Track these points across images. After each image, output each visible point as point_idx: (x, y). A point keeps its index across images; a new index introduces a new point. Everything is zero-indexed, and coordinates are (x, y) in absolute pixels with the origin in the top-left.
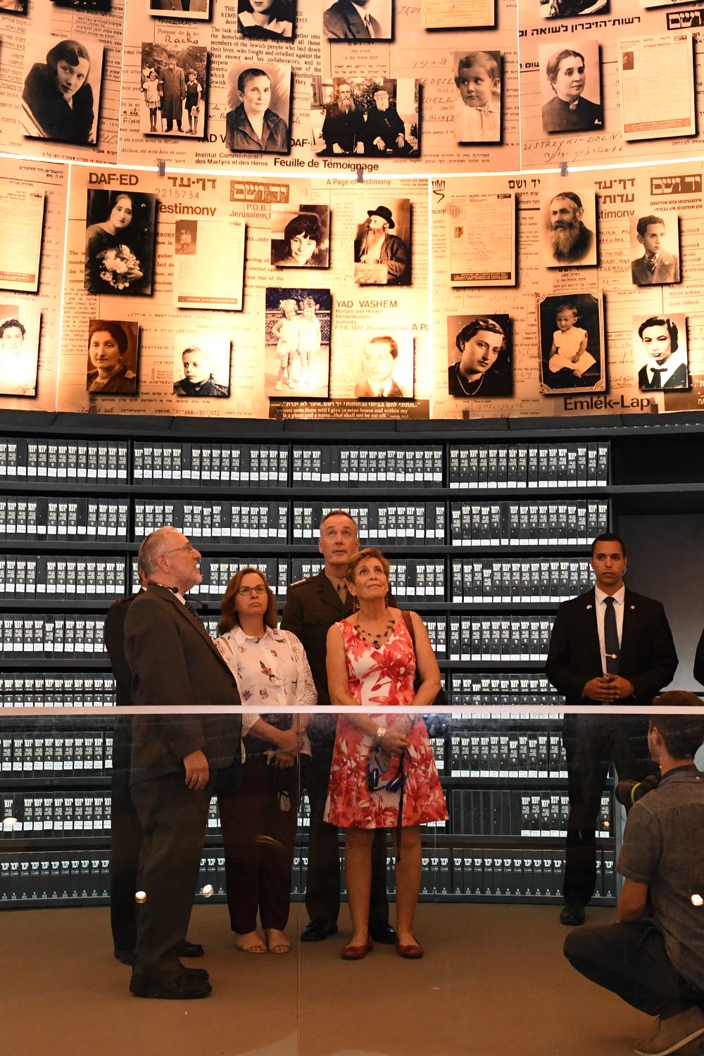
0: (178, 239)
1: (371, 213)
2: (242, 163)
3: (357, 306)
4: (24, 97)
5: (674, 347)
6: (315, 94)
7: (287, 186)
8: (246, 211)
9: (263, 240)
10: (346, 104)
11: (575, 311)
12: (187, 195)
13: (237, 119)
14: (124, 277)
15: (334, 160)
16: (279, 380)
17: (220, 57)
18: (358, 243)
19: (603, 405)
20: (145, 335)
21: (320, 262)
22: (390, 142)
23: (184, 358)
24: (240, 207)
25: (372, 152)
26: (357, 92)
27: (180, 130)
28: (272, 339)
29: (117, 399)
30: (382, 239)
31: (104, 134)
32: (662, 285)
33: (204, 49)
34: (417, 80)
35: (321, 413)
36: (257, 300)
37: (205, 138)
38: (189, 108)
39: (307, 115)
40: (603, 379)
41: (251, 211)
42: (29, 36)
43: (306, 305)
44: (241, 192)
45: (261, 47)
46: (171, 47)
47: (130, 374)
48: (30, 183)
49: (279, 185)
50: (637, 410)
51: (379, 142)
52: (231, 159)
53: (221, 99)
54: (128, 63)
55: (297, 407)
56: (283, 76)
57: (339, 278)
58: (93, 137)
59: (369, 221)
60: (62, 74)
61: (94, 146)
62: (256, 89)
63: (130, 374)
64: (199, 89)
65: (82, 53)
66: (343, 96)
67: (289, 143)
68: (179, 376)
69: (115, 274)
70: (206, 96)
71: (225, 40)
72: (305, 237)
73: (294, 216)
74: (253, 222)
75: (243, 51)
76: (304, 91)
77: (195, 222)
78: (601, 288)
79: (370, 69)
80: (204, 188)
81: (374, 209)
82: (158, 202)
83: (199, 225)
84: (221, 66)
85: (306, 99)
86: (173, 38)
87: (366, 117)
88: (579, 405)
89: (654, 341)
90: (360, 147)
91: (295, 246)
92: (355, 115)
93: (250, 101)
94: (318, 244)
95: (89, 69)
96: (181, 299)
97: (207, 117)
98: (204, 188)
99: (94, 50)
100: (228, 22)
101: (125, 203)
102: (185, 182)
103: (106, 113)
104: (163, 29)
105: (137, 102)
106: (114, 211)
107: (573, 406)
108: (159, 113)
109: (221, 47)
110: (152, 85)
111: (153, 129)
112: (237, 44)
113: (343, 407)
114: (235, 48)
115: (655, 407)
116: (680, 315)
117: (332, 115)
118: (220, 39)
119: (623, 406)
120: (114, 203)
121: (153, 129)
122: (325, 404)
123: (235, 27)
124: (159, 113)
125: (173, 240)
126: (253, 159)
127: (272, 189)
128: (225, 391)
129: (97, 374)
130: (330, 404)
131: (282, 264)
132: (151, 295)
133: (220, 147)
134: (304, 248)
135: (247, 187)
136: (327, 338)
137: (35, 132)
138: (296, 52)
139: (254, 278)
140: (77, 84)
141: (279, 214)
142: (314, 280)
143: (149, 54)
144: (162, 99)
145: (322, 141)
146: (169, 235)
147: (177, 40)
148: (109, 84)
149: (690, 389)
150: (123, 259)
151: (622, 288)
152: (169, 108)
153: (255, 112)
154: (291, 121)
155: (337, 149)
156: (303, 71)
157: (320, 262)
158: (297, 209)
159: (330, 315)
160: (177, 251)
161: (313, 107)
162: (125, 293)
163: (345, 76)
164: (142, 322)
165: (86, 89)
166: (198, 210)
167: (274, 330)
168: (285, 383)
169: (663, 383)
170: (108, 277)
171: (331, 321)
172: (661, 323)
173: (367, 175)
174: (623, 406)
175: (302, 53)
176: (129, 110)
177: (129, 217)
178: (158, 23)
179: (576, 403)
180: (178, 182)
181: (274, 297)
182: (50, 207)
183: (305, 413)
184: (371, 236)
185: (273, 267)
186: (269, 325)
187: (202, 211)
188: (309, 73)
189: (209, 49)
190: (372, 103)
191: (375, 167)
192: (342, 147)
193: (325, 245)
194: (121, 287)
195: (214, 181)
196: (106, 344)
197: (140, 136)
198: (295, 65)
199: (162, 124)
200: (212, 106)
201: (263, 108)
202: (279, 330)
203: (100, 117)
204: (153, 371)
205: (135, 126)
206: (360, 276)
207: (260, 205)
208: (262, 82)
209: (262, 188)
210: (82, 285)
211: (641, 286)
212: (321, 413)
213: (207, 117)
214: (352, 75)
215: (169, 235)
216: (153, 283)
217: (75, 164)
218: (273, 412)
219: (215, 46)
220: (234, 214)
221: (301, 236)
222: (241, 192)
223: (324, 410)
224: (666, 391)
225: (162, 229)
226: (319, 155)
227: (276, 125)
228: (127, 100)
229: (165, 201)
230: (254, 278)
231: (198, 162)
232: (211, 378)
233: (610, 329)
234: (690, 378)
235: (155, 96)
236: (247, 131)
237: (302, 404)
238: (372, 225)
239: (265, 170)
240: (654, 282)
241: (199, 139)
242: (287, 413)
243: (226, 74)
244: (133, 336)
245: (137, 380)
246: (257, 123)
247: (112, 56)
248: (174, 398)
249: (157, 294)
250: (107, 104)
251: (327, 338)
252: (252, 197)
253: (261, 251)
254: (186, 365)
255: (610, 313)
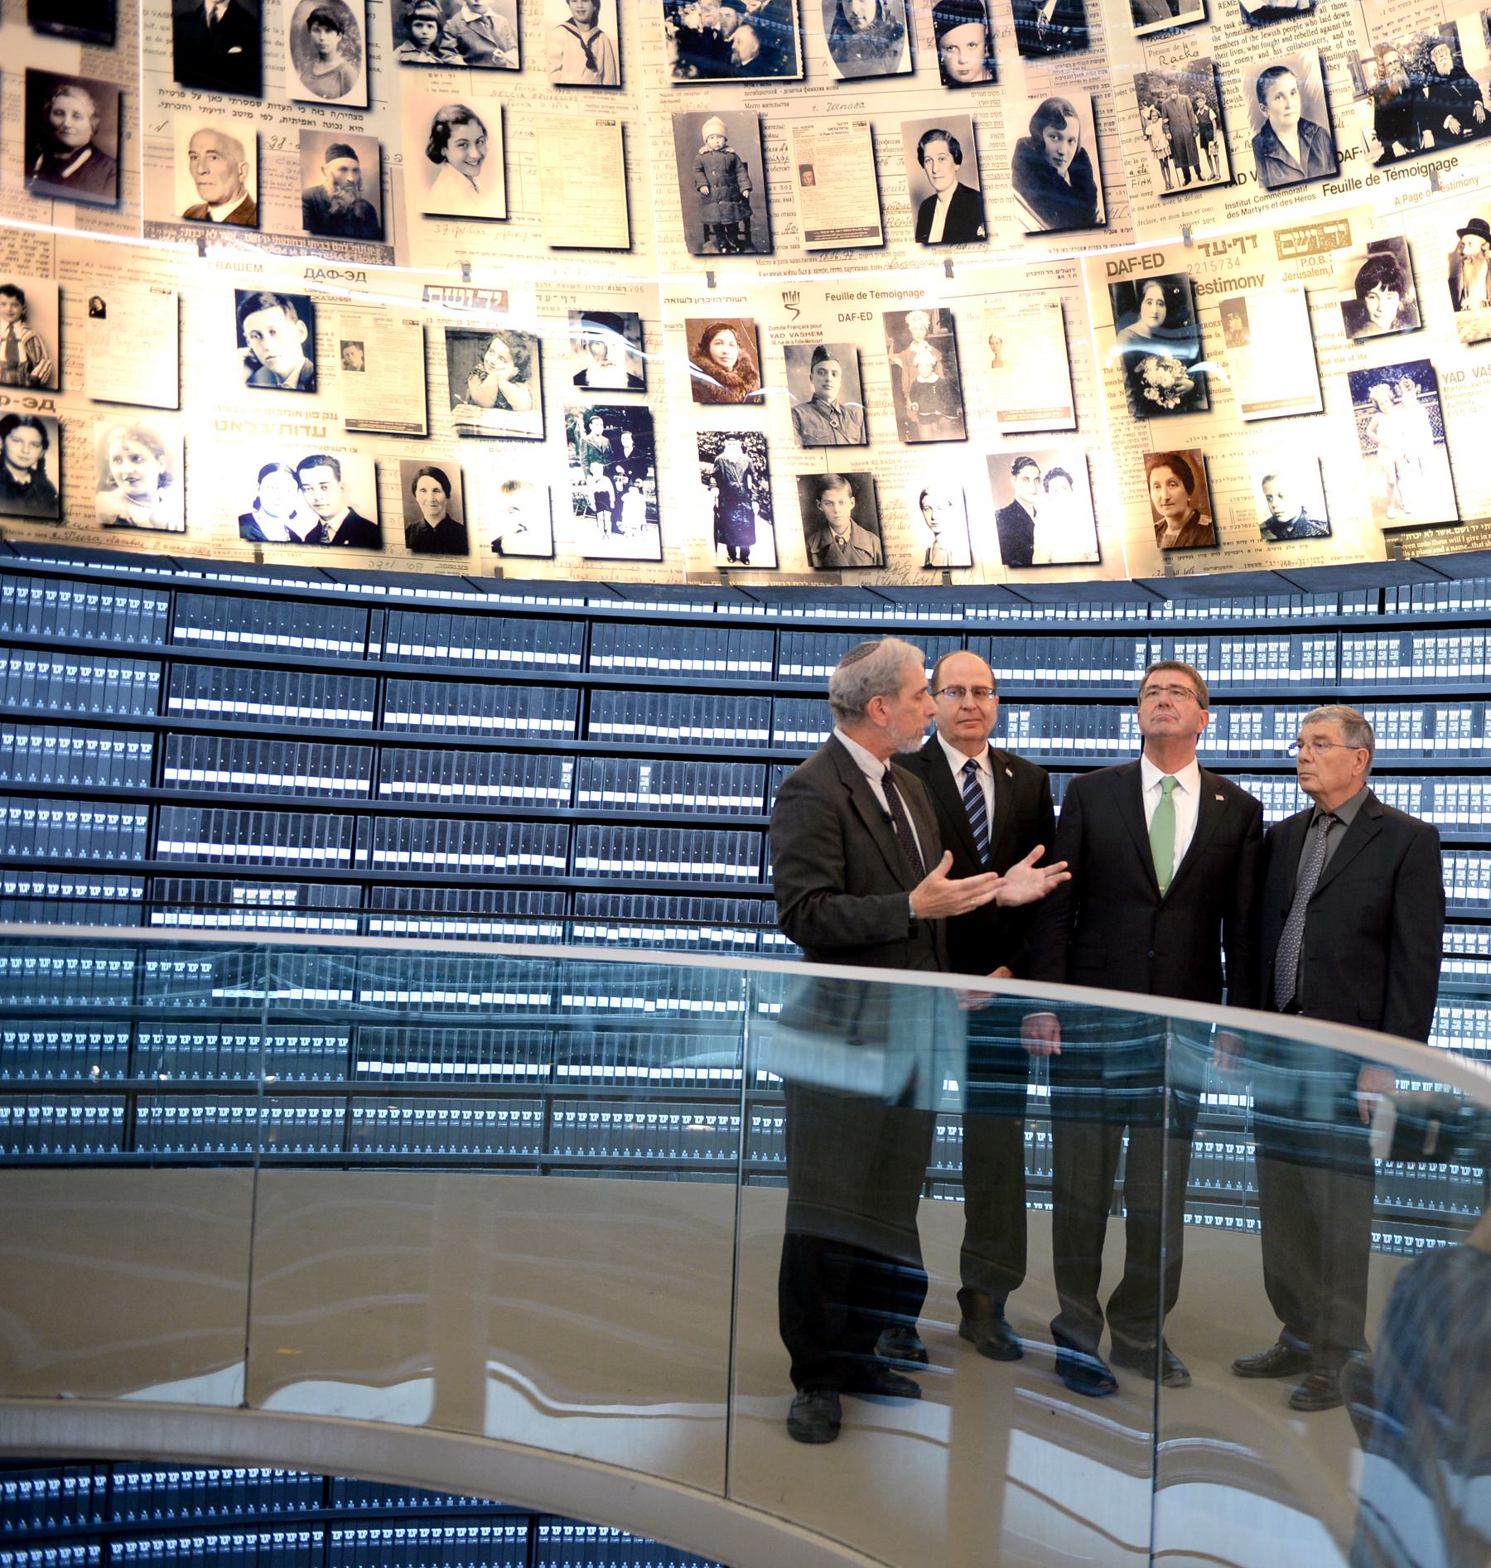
0: (1226, 328)
1: (1462, 233)
2: (1284, 203)
3: (1470, 378)
4: (1015, 185)
6: (1355, 79)
7: (1345, 221)
8: (1302, 270)
9: (1330, 305)
10: (1397, 80)
12: (1226, 264)
13: (1266, 143)
14: (1173, 390)
15: (1398, 167)
16: (1389, 503)
17: (1228, 63)
18: (1453, 282)
20: (1212, 464)
21: (1409, 319)
22: (1466, 119)
23: (1265, 489)
24: (1292, 265)
25: (1446, 140)
26: (1408, 58)
27: (1200, 178)
28: (1370, 447)
29: (1196, 554)
30: (1485, 267)
31: (1112, 207)
33: (1206, 61)
34: (1483, 13)
35: (1454, 544)
36: (1340, 391)
37: (1232, 182)
38: (1205, 145)
39: (1352, 112)
41: (1307, 268)
42: (1005, 107)
43: (1404, 389)
44: (1289, 244)
45: (1275, 33)
46: (1168, 71)
47: (1205, 520)
48: (1042, 291)
49: (1335, 223)
51: (1451, 124)
52: (1269, 202)
53: (1241, 124)
54: (1123, 106)
55: (1421, 540)
56: (1309, 67)
57: (1440, 340)
58: (1101, 216)
59: (1461, 245)
60: (1051, 145)
61: (1103, 226)
62: (1281, 95)
63: (1205, 520)
64: (1213, 116)
65: (1068, 111)
66: (1390, 69)
67: (1336, 157)
68: (1264, 516)
69: (1161, 389)
70: (1222, 123)
71: (1232, 39)
72: (1383, 289)
73: (1363, 262)
74: (1311, 283)
75: (1255, 48)
76: (1341, 78)
77: (1241, 301)
79: (1419, 18)
80: (1244, 251)
81: (1465, 226)
82: (1193, 283)
83: (1248, 303)
84: (1232, 77)
85: (1346, 90)
86: (1168, 57)
87: (1426, 91)
90: (1428, 139)
91: (1371, 304)
92: (1413, 90)
93: (1277, 113)
94: (1402, 296)
95: (1079, 128)
96: (1246, 408)
97: (1229, 151)
98: (1244, 251)
99: (1080, 103)
100: (1229, 14)
101: (1154, 293)
102: (1220, 248)
103: (1109, 181)
104: (1154, 49)
105: (1143, 155)
106: (1144, 306)
108: (1171, 163)
109: (1227, 50)
110: (1156, 127)
111: (1169, 186)
112: (1245, 41)
113: (1481, 531)
114: (1243, 46)
117: (1383, 102)
118: (1224, 40)
120: (1142, 296)
121: (1169, 186)
122: (1457, 530)
123: (1238, 18)
124: (1171, 163)
125: (1220, 329)
126: (1296, 195)
127: (1328, 230)
128: (1324, 528)
129: (1165, 524)
130: (1462, 530)
131: (1361, 334)
132: (1209, 410)
133: (1251, 189)
134: (1383, 304)
135: (1296, 235)
136: (1440, 432)
137: (1036, 227)
138: (1320, 26)
139: (1329, 362)
140: (1069, 152)
141: (1348, 262)
142: (1406, 349)
143: (1144, 89)
144: (1172, 143)
145: (1378, 143)
146: (1214, 324)
147: (1172, 59)
148: (1105, 142)
150: (1166, 367)
152: (1182, 155)
153: (1286, 127)
154: (1332, 127)
155: (1398, 149)
156: (1334, 51)
157: (1409, 319)
158: (1365, 251)
159: (1437, 397)
160: (1229, 343)
161: (1357, 98)
162: (1178, 411)
163: (1388, 40)
164: (1206, 449)
165: (1081, 157)
166: (1242, 283)
167: (1369, 432)
168: (1399, 506)
170: (1152, 395)
171: (1440, 406)
173: (1444, 176)
175: (1327, 24)
176: (1135, 168)
177: (1163, 311)
178: (1147, 43)
180: (1211, 249)
181: (1361, 385)
182: (1070, 317)
183: (1433, 546)
184: (1468, 268)
185: (1351, 341)
186: (1362, 425)
187: (1248, 281)
188: (1341, 51)
189: (1213, 59)
190: (1430, 68)
191: (1454, 162)
192: (1405, 145)
193: (1410, 295)
194: (1171, 405)
195: (1254, 237)
196: (1169, 483)
197: (1155, 199)
198: (1322, 45)
199: (1177, 175)
200: (1232, 136)
201: (1294, 119)
202: (1375, 431)
203: (1104, 188)
204: (1231, 510)
205: (1146, 188)
206: (1464, 332)
207: (1316, 256)
208: (1285, 83)
209: (1314, 232)
210: (1125, 411)
212: (1454, 544)
213: (1229, 151)
214: (1397, 34)
215: (1214, 324)
216: (1208, 393)
217: (1085, 253)
218: (1394, 550)
219: (1220, 52)
220: (1288, 277)
221: (1377, 290)
222: (1289, 244)
223: (1458, 539)
225: (1205, 317)
226: (1378, 165)
227: (1315, 137)
228: (1131, 159)
229: (1202, 280)
230: (1329, 362)
231: (1230, 216)
232: (1304, 512)
235: (1162, 141)
236: (1281, 157)
237: (1427, 534)
238: (1467, 251)
239: (1313, 205)
241: (1225, 185)
242: (1410, 550)
243: (1240, 86)
244: (1198, 468)
245: (1214, 525)
246: (1290, 140)
247: (1102, 105)
248: (1264, 545)
249: (1216, 407)
250: (1108, 168)
251: (1440, 432)
252: (1304, 248)
253: (1332, 322)
254: (1269, 498)
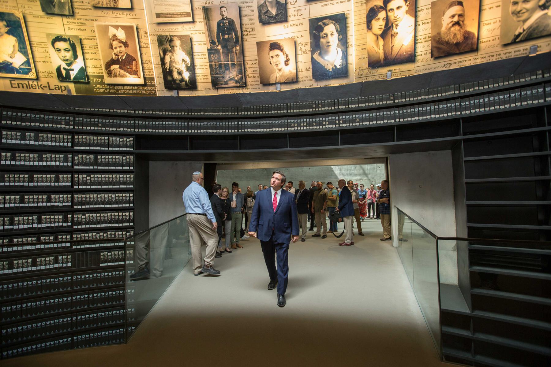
5: (75, 57)
11: (5, 23)
19: (37, 87)
32: (62, 15)
40: (34, 71)
50: (59, 92)
78: (20, 10)
88: (20, 85)
89: (63, 51)
107: (17, 85)
115: (69, 91)
116: (76, 37)
119: (50, 89)
149: (88, 83)
151: (35, 13)
169: (72, 77)
172: (64, 40)
174: (50, 89)
179: (18, 84)
211: (48, 14)
224: (75, 83)
233: (33, 39)
234: (88, 76)
240: (56, 13)
255: (31, 29)
